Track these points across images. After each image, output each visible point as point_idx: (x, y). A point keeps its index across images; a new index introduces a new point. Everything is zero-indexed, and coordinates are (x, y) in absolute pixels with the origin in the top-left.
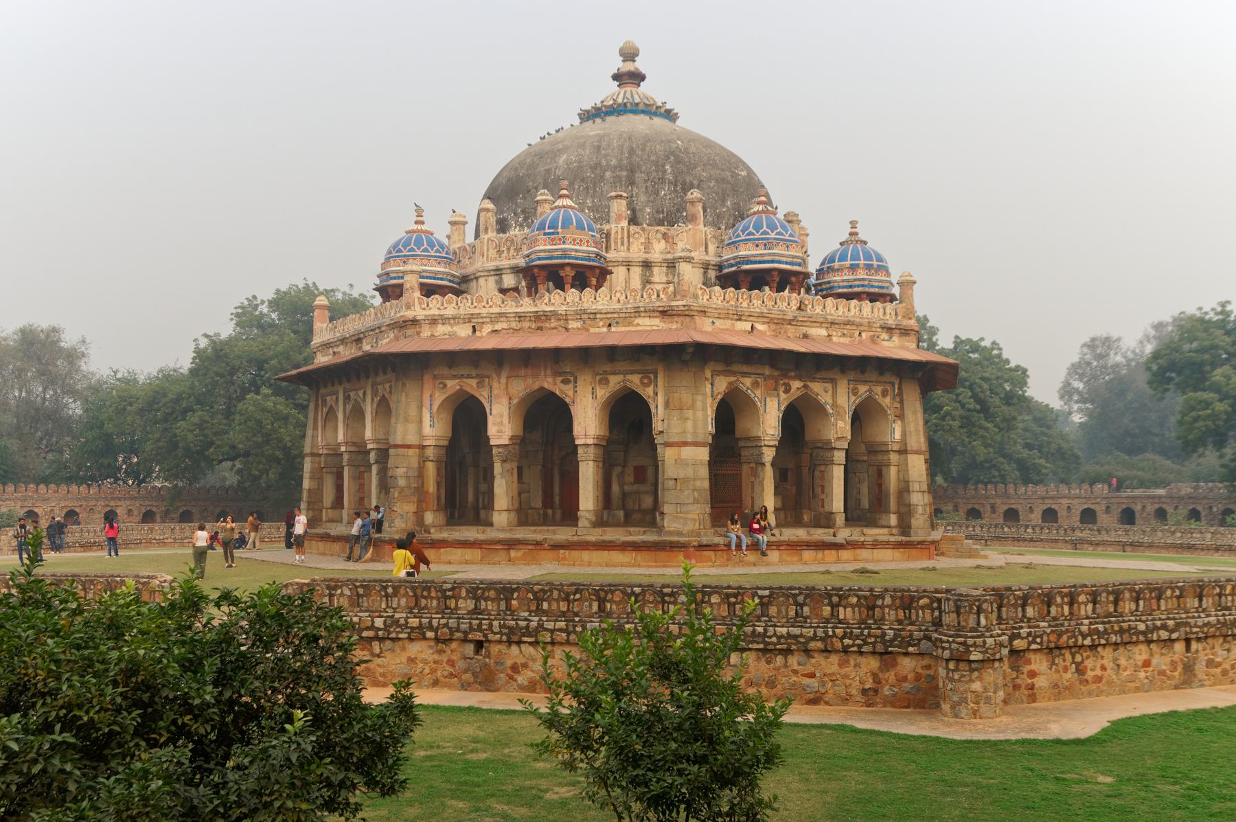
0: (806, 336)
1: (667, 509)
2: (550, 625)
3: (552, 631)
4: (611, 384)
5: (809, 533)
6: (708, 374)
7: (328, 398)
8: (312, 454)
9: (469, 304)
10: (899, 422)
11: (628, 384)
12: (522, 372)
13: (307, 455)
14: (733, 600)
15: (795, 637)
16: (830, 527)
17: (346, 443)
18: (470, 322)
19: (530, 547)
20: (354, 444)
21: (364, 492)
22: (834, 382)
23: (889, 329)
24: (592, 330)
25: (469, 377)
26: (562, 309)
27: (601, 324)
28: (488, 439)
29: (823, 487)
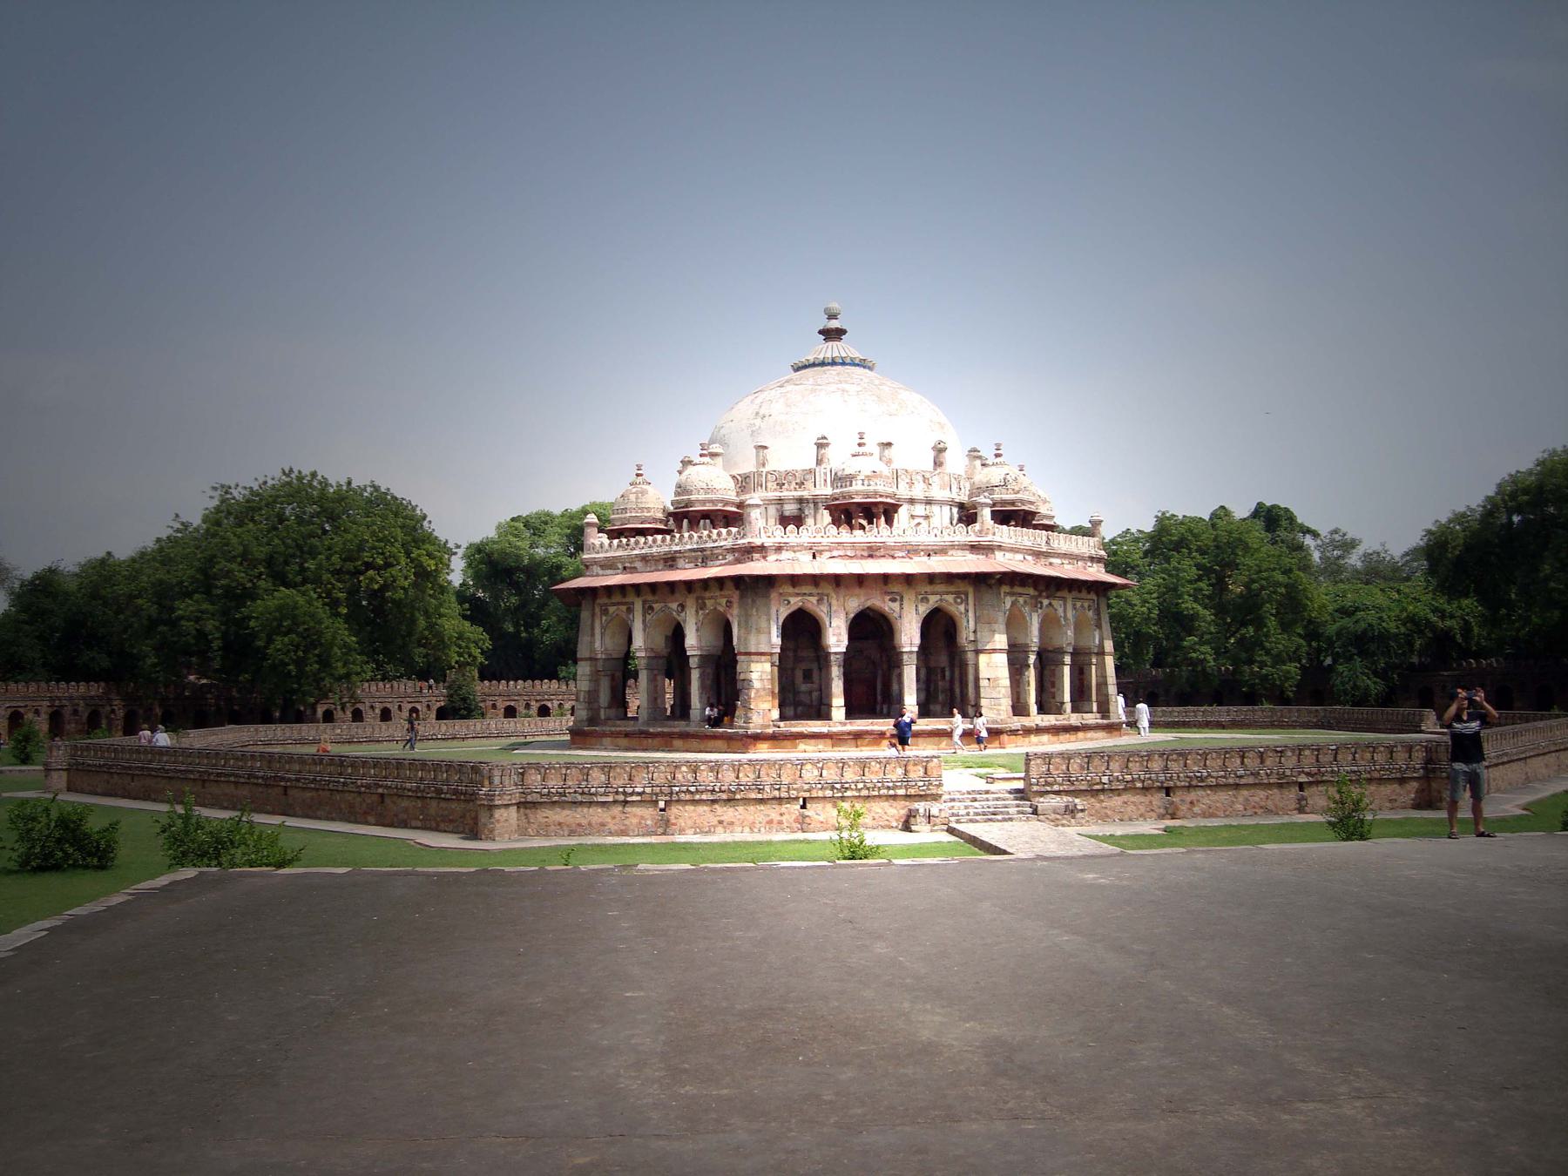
0: (1051, 564)
1: (983, 702)
2: (1214, 774)
3: (1217, 778)
4: (931, 602)
5: (1057, 720)
6: (1002, 594)
7: (612, 609)
8: (591, 659)
9: (810, 534)
10: (1098, 630)
11: (944, 604)
12: (857, 591)
13: (582, 659)
14: (1316, 753)
15: (1355, 772)
16: (1061, 714)
17: (646, 650)
18: (810, 549)
19: (873, 736)
20: (652, 649)
21: (657, 693)
22: (1064, 599)
23: (1092, 559)
24: (916, 559)
25: (811, 595)
26: (890, 541)
27: (922, 553)
28: (829, 646)
29: (1053, 685)
